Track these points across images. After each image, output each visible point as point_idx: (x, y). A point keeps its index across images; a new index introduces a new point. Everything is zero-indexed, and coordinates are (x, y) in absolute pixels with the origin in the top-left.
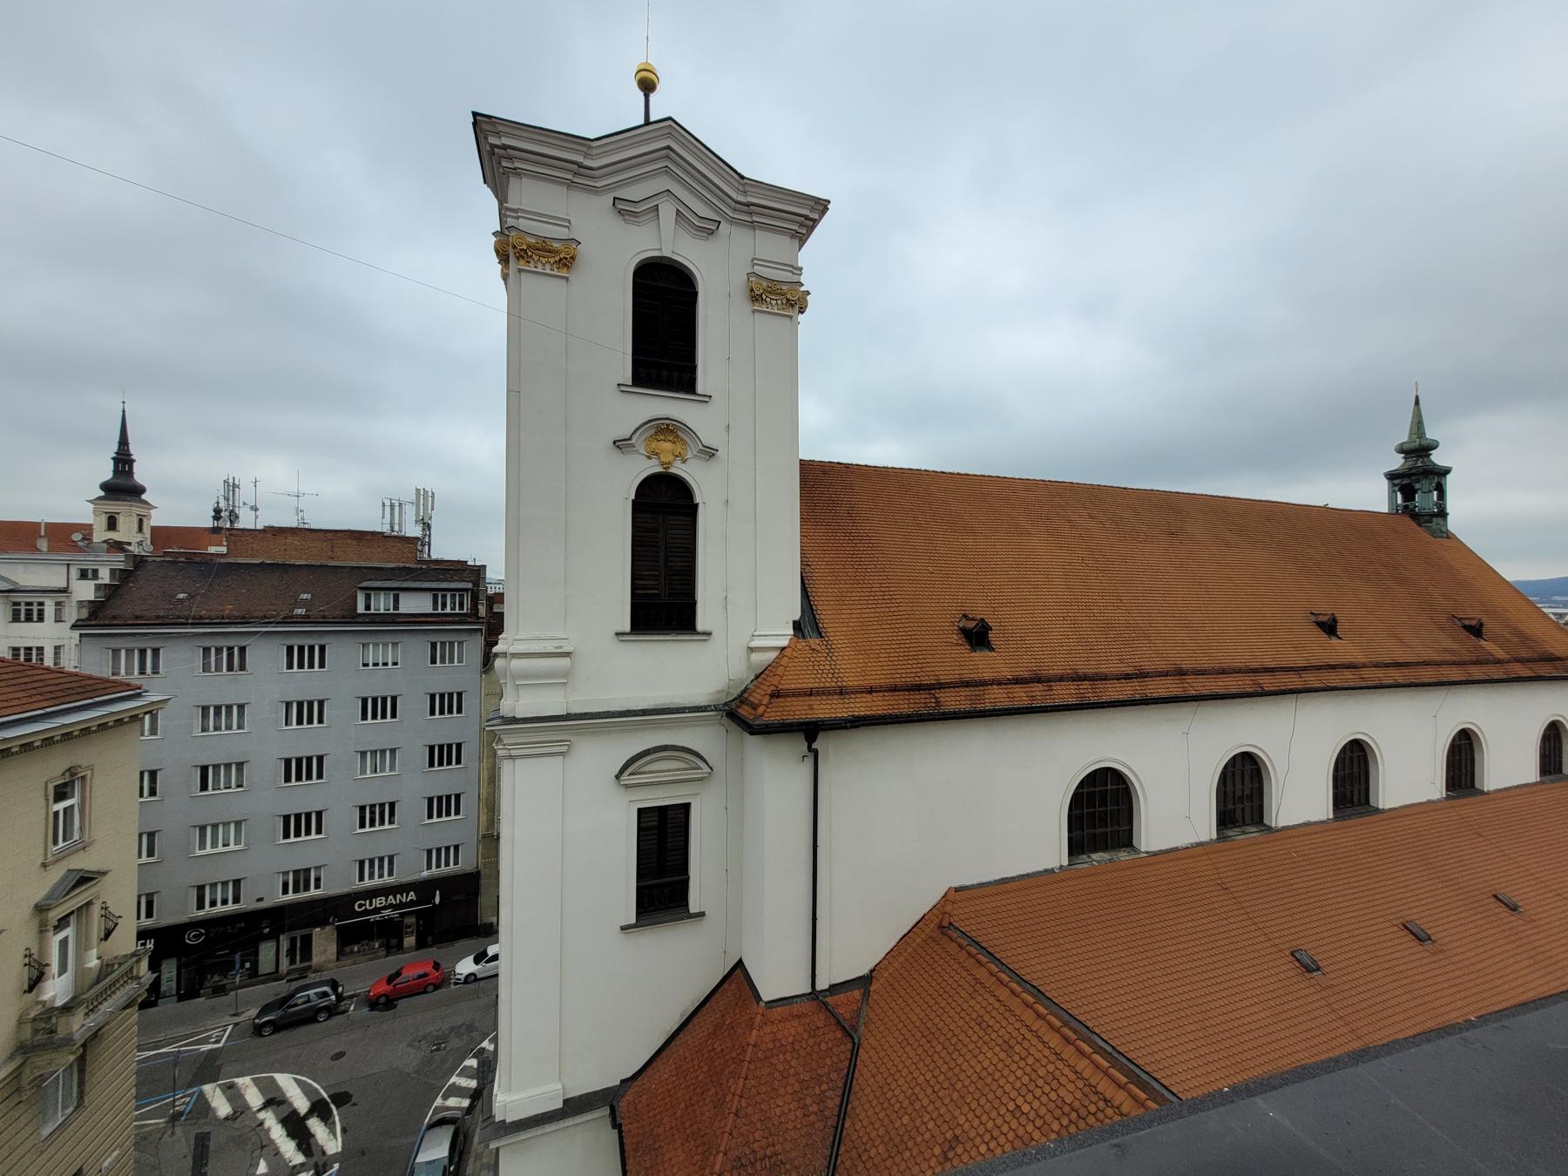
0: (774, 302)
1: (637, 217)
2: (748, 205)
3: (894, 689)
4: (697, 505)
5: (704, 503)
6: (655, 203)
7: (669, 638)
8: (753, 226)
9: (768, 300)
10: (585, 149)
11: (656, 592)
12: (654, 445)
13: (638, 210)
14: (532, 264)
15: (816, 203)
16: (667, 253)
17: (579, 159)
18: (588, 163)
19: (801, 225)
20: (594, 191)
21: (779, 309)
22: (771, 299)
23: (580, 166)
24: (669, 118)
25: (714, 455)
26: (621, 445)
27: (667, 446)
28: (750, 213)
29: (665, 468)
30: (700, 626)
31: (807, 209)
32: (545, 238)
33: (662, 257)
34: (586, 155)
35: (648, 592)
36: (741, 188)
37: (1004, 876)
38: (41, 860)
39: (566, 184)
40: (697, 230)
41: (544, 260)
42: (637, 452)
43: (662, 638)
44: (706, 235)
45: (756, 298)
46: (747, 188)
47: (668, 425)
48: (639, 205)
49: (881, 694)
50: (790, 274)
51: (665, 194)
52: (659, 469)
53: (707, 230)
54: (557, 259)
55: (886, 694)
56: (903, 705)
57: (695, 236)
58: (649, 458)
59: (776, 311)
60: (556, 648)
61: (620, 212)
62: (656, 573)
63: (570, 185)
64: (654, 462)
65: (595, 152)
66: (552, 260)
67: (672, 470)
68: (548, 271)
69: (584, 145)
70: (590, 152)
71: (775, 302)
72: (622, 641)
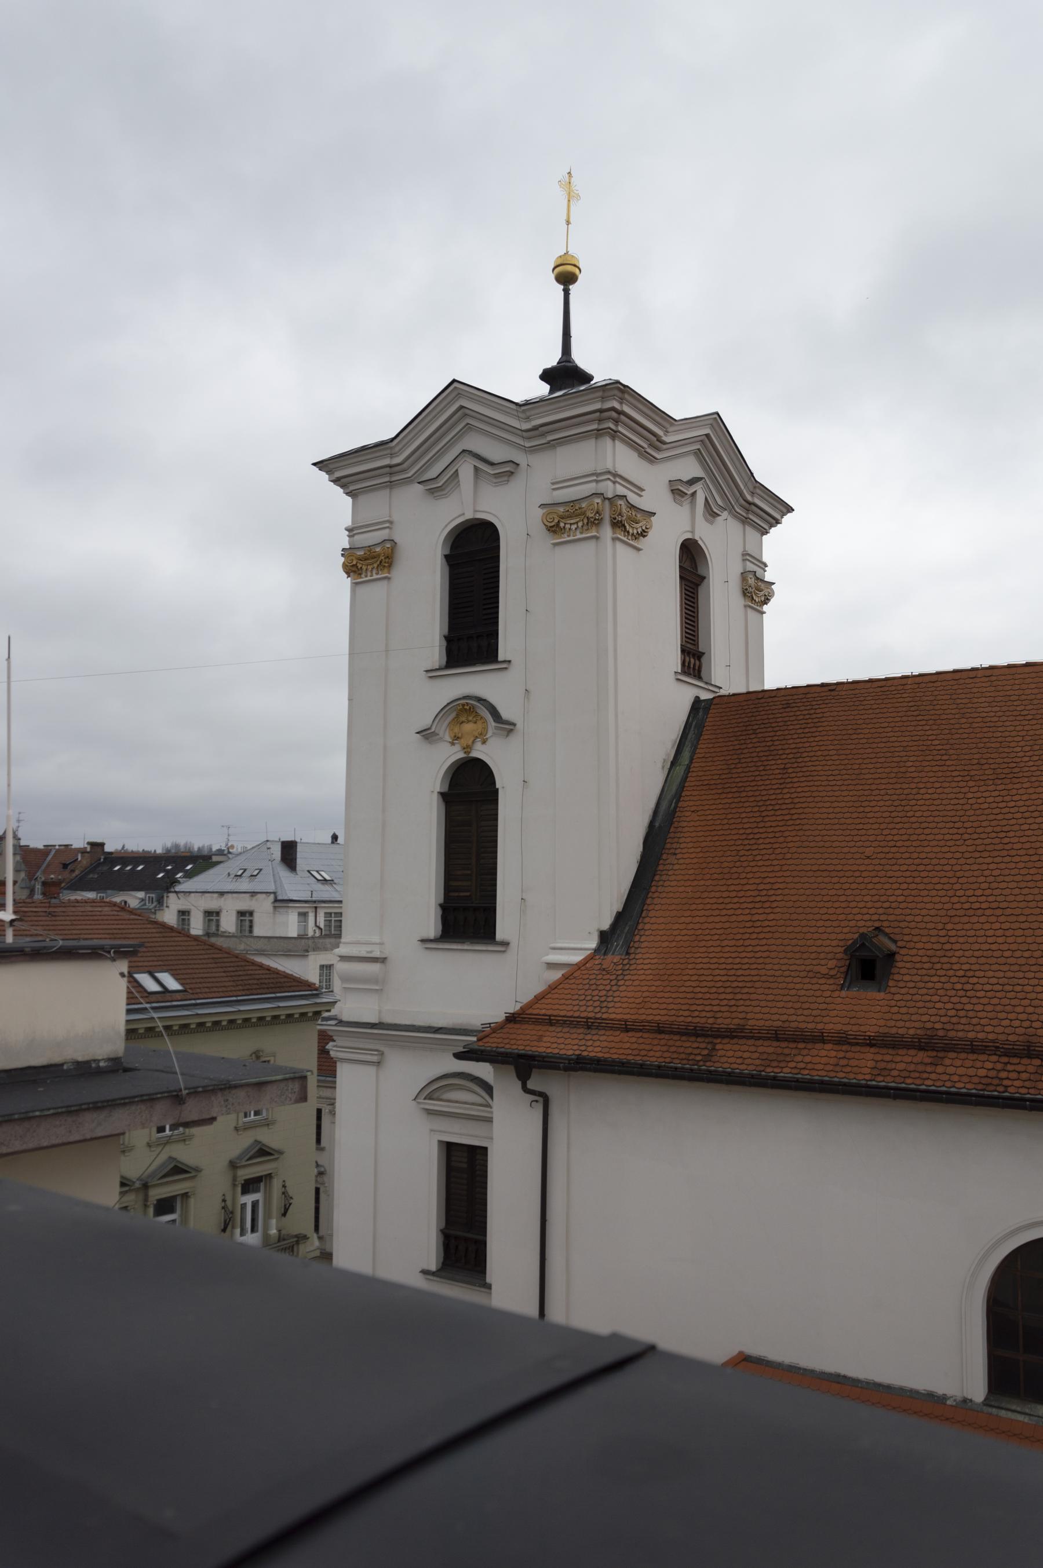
0: (574, 527)
1: (443, 490)
2: (535, 428)
3: (660, 1029)
4: (498, 789)
5: (503, 787)
6: (454, 470)
7: (466, 947)
8: (552, 445)
9: (568, 526)
10: (388, 451)
11: (468, 894)
12: (456, 730)
13: (439, 485)
14: (363, 576)
15: (604, 391)
16: (469, 515)
17: (387, 461)
18: (397, 460)
19: (600, 420)
20: (408, 481)
21: (581, 533)
22: (571, 524)
23: (390, 466)
24: (454, 381)
25: (511, 730)
26: (427, 734)
27: (468, 727)
28: (543, 435)
29: (465, 753)
30: (499, 936)
31: (597, 402)
32: (369, 546)
33: (467, 520)
34: (392, 455)
35: (462, 894)
36: (520, 415)
37: (843, 1372)
38: (234, 1124)
39: (387, 486)
40: (496, 478)
41: (370, 568)
42: (441, 739)
43: (459, 947)
44: (506, 478)
45: (554, 529)
46: (528, 414)
47: (463, 705)
48: (438, 480)
49: (640, 1034)
50: (594, 484)
51: (464, 454)
52: (461, 755)
53: (506, 472)
54: (378, 562)
55: (646, 1035)
56: (656, 1051)
57: (497, 484)
58: (453, 744)
59: (579, 536)
60: (368, 952)
61: (432, 491)
62: (469, 872)
63: (391, 485)
64: (457, 747)
65: (397, 449)
66: (375, 565)
67: (474, 754)
68: (375, 577)
69: (387, 448)
70: (393, 452)
71: (575, 526)
72: (426, 948)
